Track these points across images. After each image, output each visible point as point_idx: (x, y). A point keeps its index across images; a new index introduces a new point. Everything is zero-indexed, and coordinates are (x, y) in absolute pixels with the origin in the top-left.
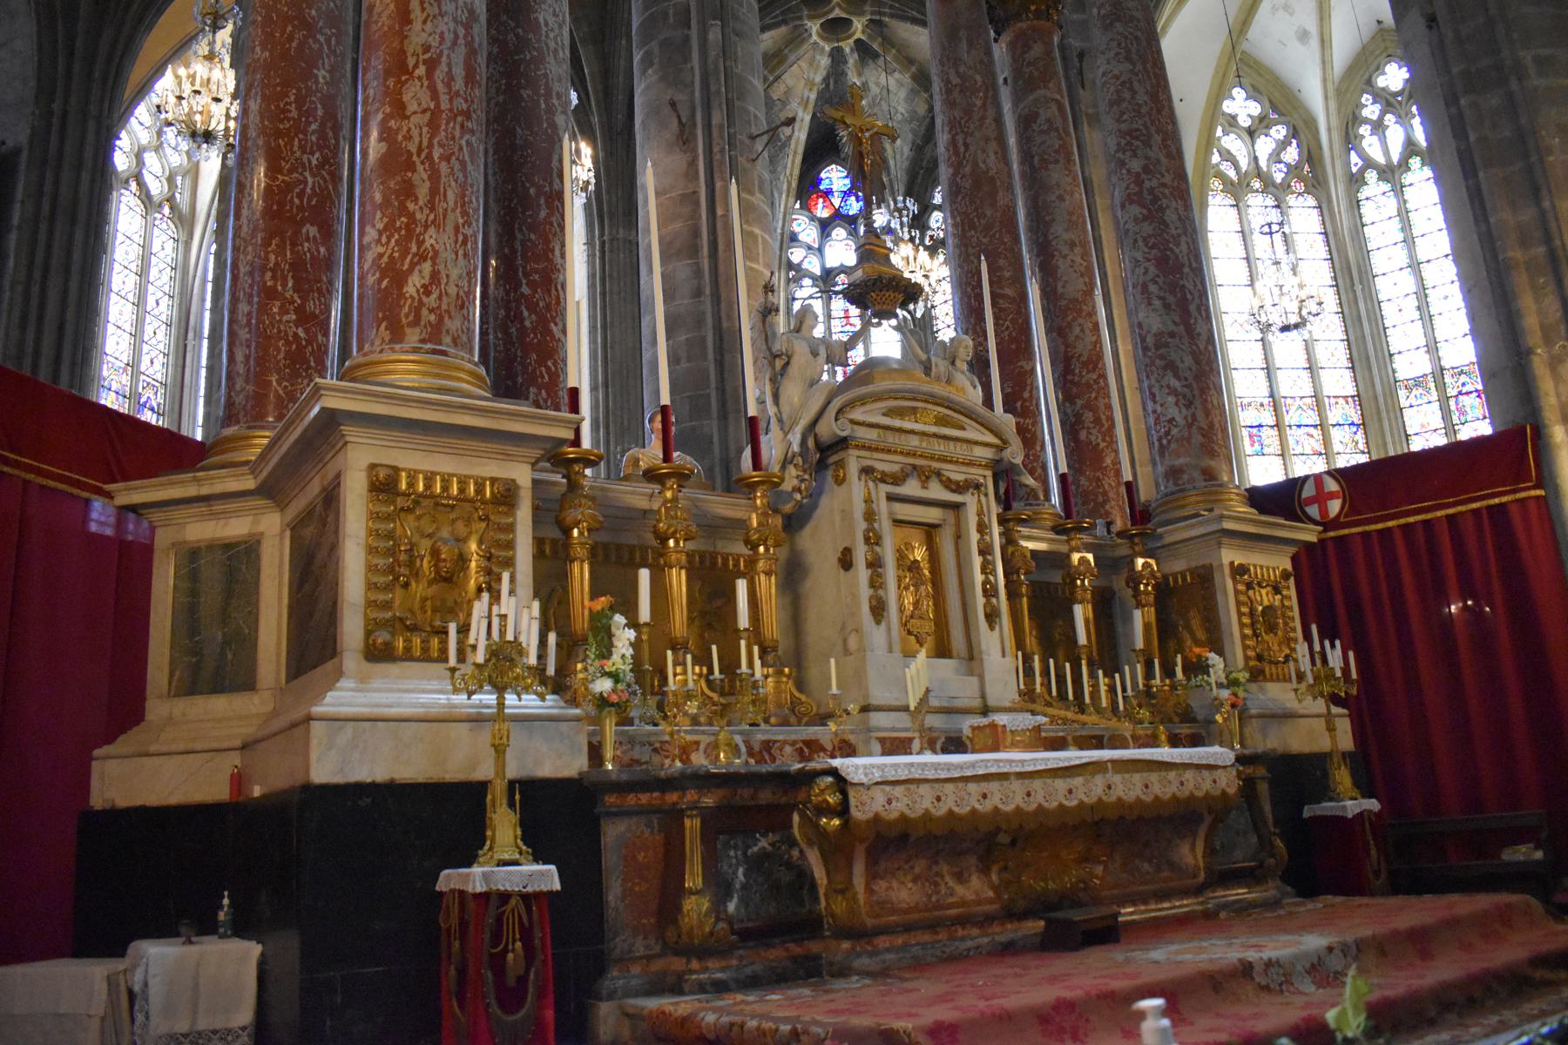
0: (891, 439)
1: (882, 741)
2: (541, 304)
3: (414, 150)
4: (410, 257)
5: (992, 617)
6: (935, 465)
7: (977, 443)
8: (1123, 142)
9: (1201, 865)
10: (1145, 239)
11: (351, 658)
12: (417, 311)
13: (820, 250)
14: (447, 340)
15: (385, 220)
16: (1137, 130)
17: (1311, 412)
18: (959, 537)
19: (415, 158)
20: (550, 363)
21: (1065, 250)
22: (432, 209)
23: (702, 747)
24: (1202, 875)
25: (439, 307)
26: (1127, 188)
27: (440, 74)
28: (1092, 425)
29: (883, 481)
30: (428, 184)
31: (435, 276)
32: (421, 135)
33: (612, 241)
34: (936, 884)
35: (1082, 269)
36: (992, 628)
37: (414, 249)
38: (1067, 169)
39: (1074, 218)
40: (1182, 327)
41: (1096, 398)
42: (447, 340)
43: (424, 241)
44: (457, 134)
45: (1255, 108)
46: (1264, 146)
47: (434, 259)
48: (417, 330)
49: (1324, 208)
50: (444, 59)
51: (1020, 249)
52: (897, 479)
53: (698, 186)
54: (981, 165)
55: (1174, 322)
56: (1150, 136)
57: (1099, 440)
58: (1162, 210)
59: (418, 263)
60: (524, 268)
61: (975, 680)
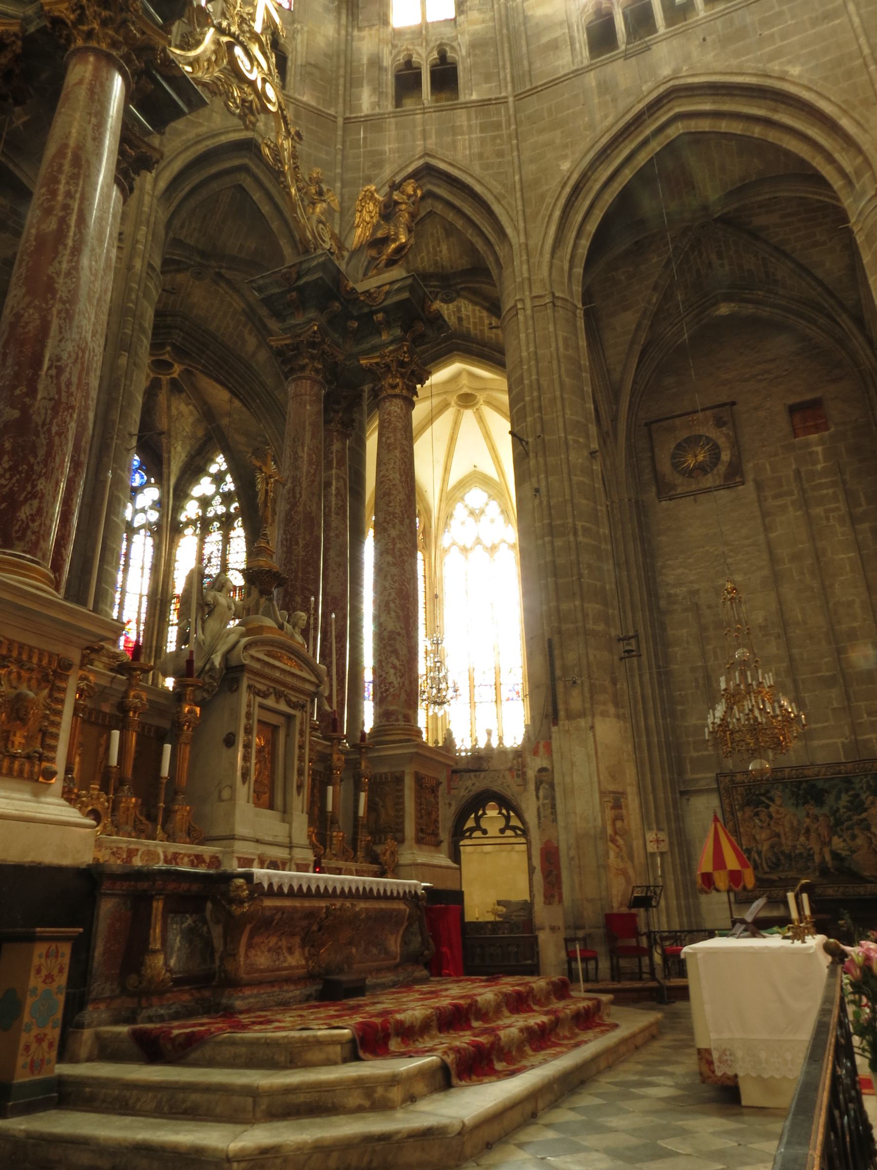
0: (267, 670)
1: (239, 859)
3: (40, 423)
4: (25, 493)
5: (300, 787)
6: (287, 691)
12: (25, 529)
15: (11, 463)
19: (39, 428)
23: (140, 853)
25: (38, 532)
26: (387, 544)
27: (64, 378)
29: (259, 696)
30: (45, 448)
32: (46, 414)
37: (29, 488)
42: (40, 554)
43: (36, 485)
50: (68, 369)
52: (265, 696)
56: (403, 519)
59: (31, 498)
61: (287, 826)
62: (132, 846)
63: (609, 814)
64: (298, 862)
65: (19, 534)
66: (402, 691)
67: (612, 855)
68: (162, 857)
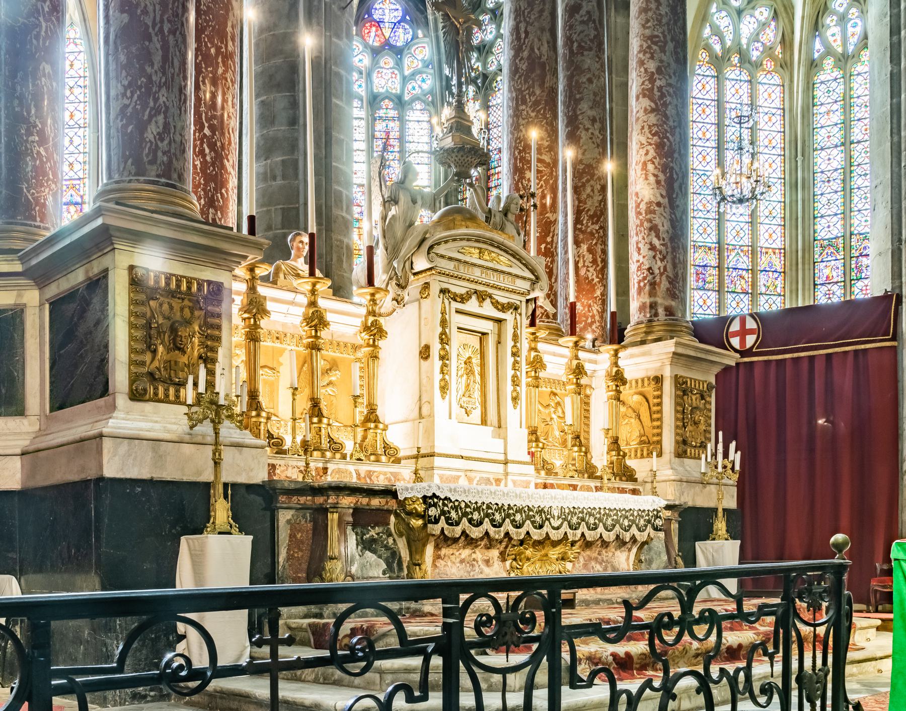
2: (219, 144)
3: (150, 24)
4: (148, 110)
6: (490, 291)
7: (517, 276)
14: (175, 176)
15: (129, 78)
19: (151, 30)
20: (223, 191)
22: (164, 73)
25: (169, 151)
28: (590, 265)
29: (455, 300)
30: (160, 52)
31: (166, 125)
32: (154, 11)
36: (515, 407)
38: (597, 56)
39: (598, 99)
40: (666, 200)
41: (596, 244)
43: (158, 98)
47: (165, 113)
48: (155, 167)
51: (557, 124)
52: (463, 299)
55: (662, 195)
57: (594, 277)
59: (155, 115)
60: (206, 114)
65: (150, 158)
66: (664, 277)
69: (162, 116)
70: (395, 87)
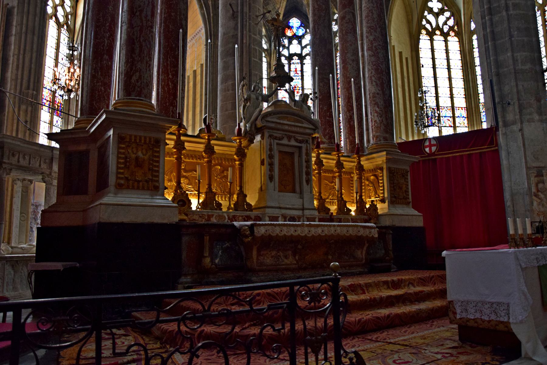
0: (279, 126)
1: (269, 217)
2: (175, 81)
8: (368, 30)
9: (364, 258)
10: (372, 62)
11: (112, 188)
13: (288, 48)
14: (143, 96)
16: (373, 26)
17: (450, 112)
18: (300, 156)
19: (135, 41)
21: (351, 62)
22: (140, 57)
24: (364, 261)
27: (143, 15)
31: (140, 77)
33: (214, 45)
34: (279, 259)
35: (356, 69)
36: (308, 184)
37: (134, 69)
40: (381, 92)
42: (143, 96)
44: (148, 33)
45: (440, 5)
46: (442, 19)
49: (461, 42)
53: (238, 32)
54: (323, 35)
55: (379, 90)
58: (378, 53)
60: (170, 70)
61: (301, 200)
62: (210, 214)
63: (533, 180)
64: (308, 216)
66: (382, 125)
67: (535, 203)
68: (227, 217)
69: (138, 73)
70: (299, 52)
